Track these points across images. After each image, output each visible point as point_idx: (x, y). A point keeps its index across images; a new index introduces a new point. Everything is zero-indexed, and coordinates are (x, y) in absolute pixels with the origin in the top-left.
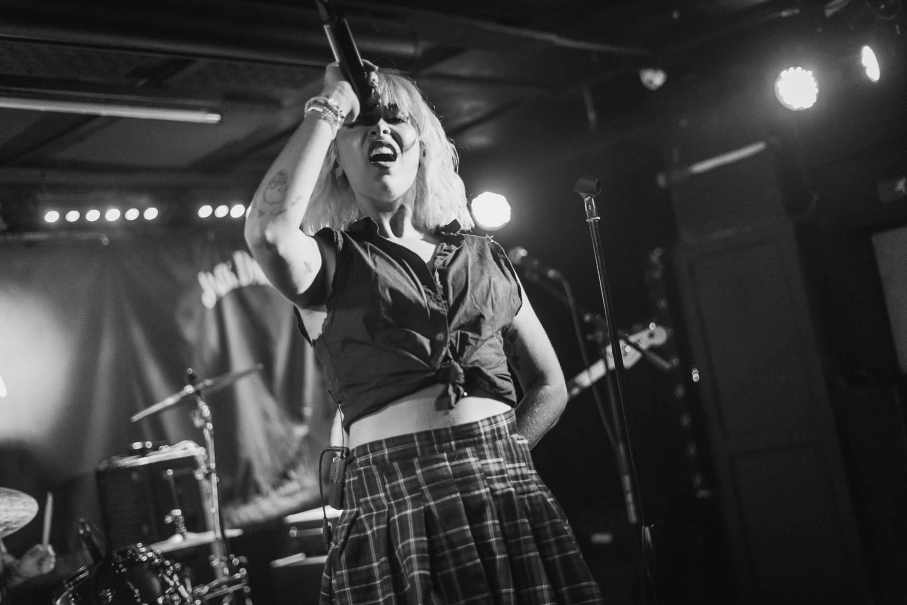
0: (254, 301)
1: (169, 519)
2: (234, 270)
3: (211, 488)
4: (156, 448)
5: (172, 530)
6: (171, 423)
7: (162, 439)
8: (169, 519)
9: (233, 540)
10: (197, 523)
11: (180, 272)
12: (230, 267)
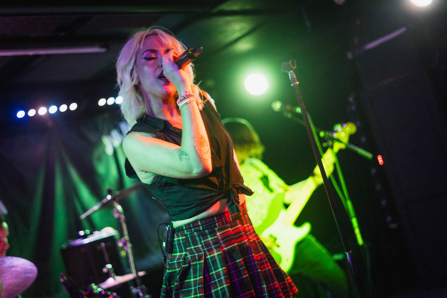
1: (105, 270)
3: (126, 251)
4: (91, 233)
5: (107, 276)
6: (97, 218)
7: (94, 228)
8: (105, 270)
9: (143, 277)
10: (120, 270)
11: (92, 136)
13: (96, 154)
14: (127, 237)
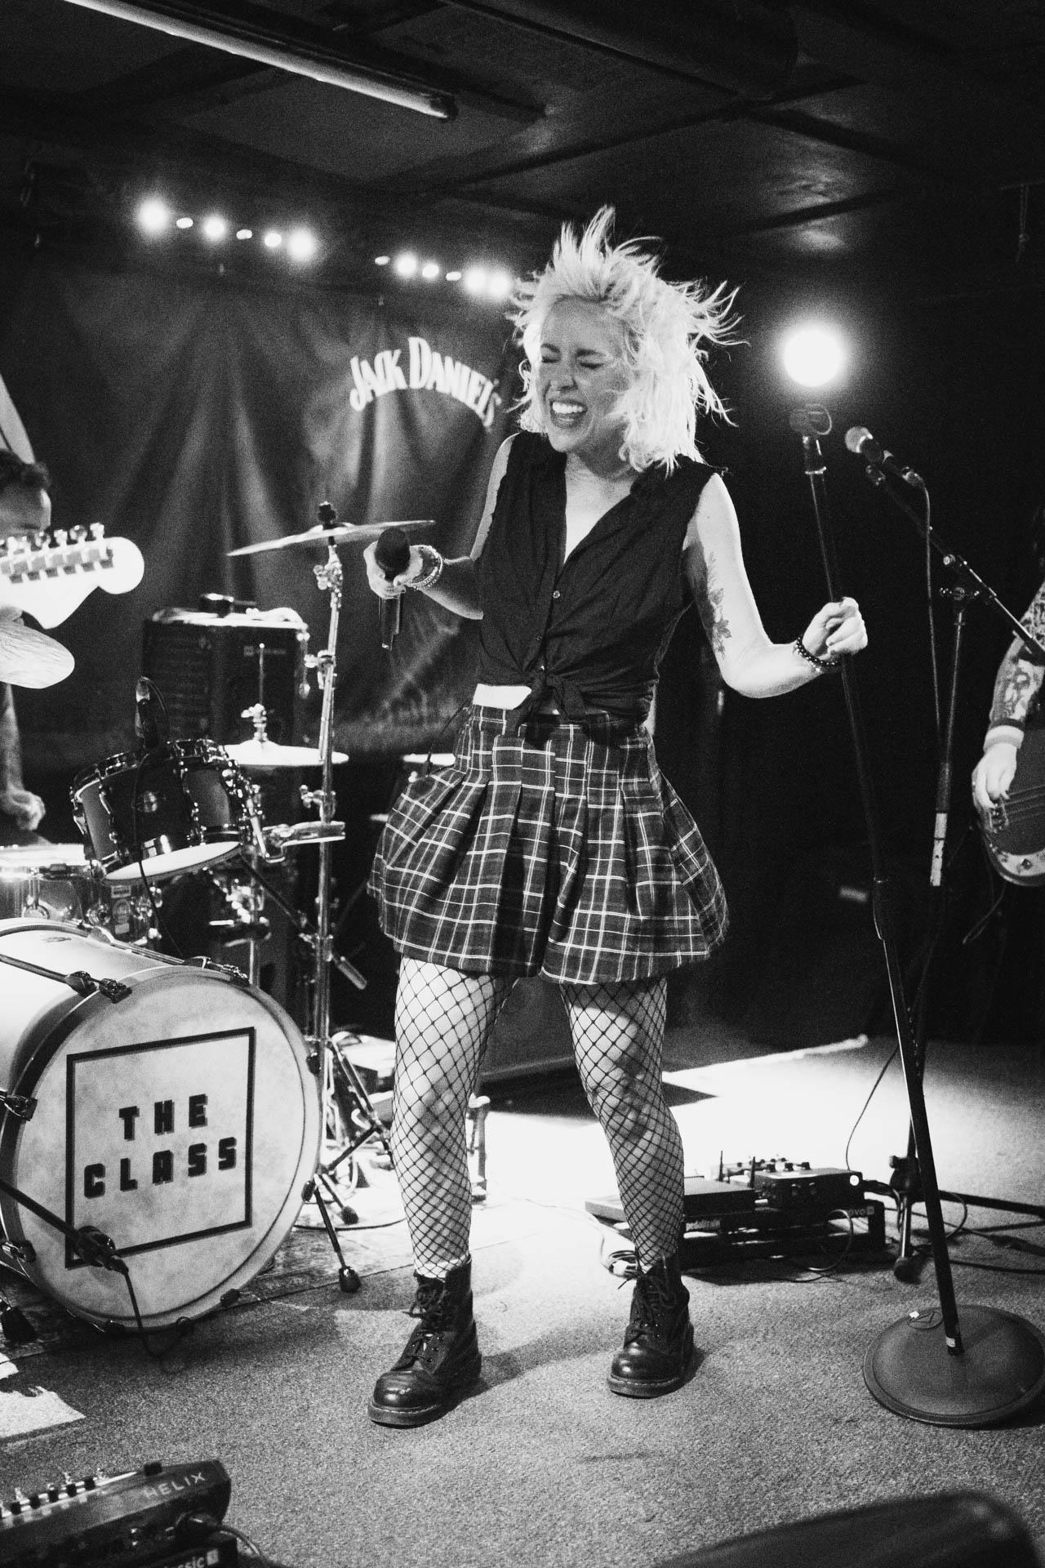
0: (423, 418)
1: (245, 714)
2: (404, 362)
4: (241, 609)
8: (245, 714)
9: (336, 768)
10: (280, 733)
12: (398, 352)
13: (318, 399)
14: (331, 651)
